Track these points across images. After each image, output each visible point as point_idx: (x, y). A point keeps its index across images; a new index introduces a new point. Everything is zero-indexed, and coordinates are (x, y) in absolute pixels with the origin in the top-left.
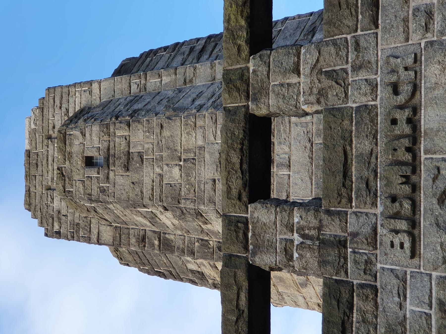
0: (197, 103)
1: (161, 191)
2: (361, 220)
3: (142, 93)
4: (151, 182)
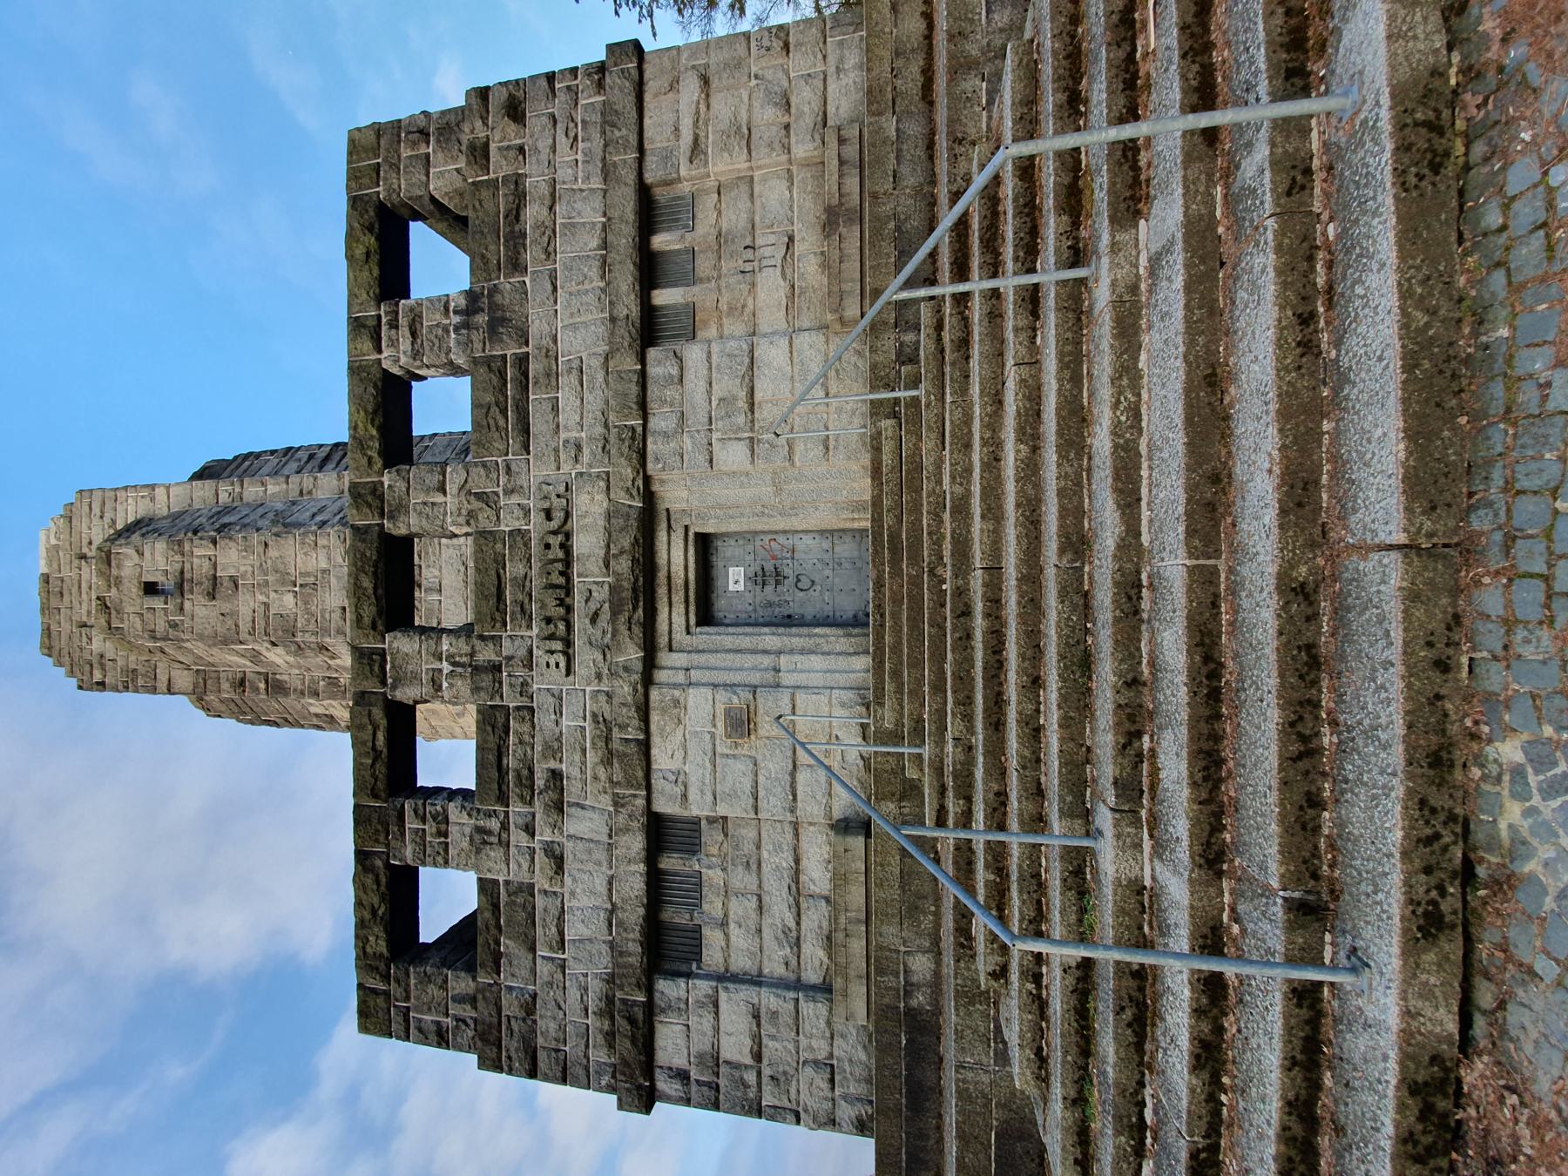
0: (319, 518)
1: (267, 623)
2: (516, 643)
3: (235, 504)
4: (251, 613)
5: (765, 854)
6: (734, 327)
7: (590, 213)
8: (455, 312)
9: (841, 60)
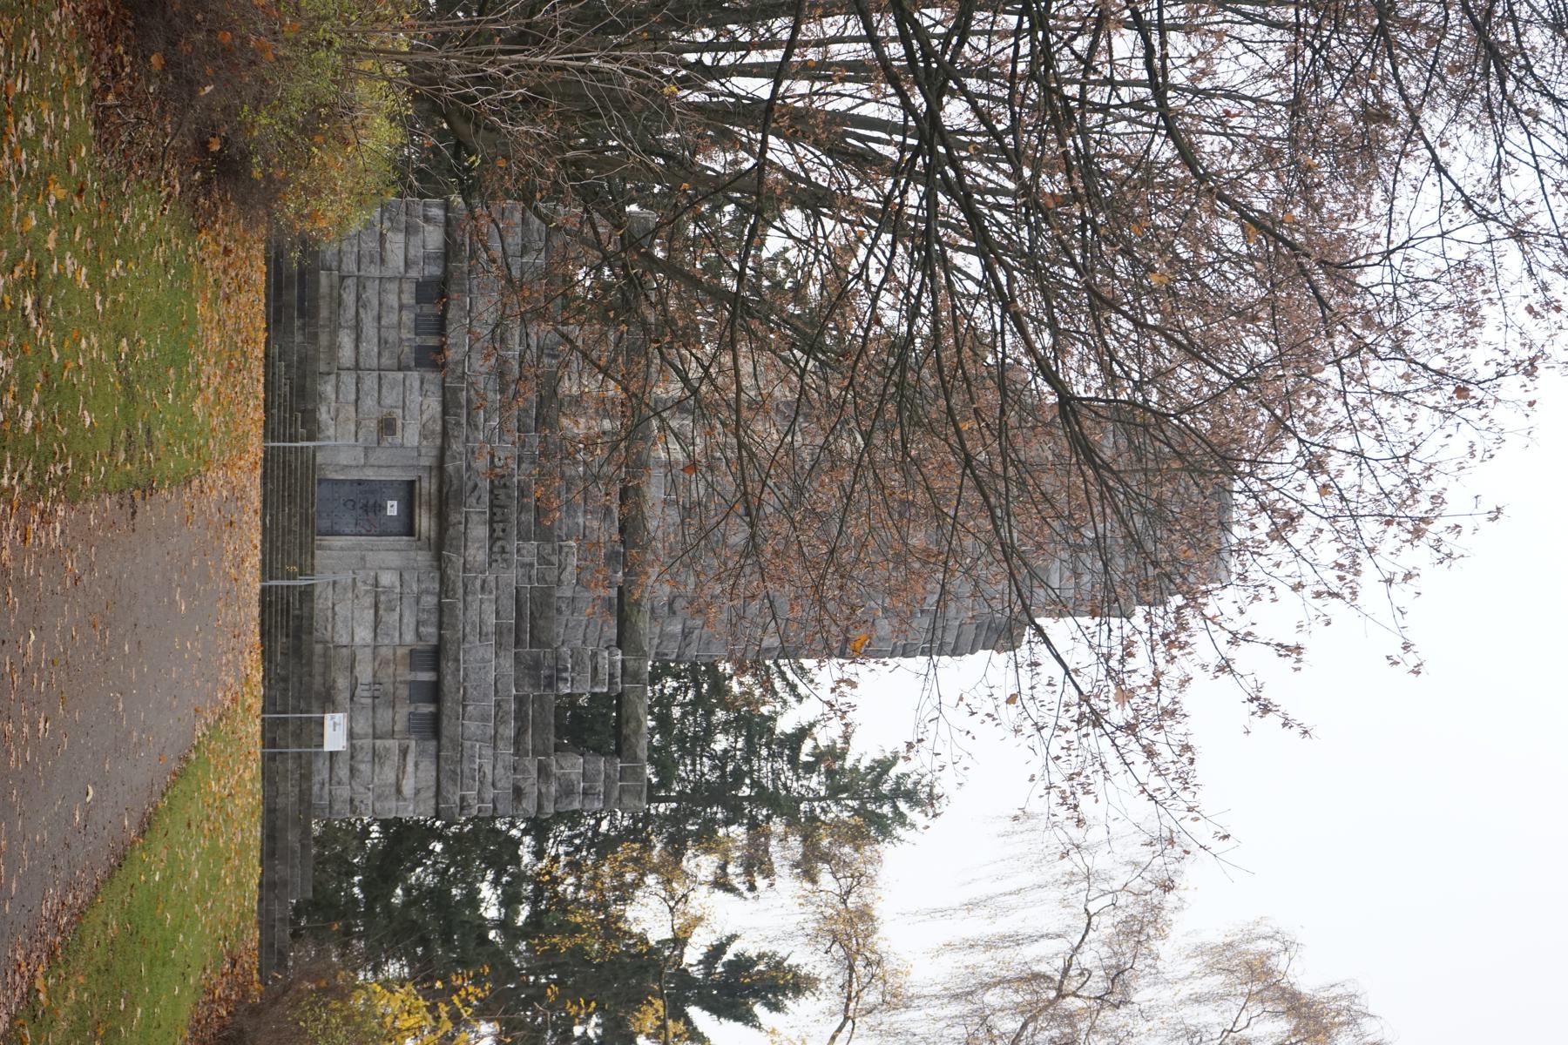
5: (376, 349)
6: (385, 652)
7: (472, 727)
8: (566, 679)
9: (322, 788)
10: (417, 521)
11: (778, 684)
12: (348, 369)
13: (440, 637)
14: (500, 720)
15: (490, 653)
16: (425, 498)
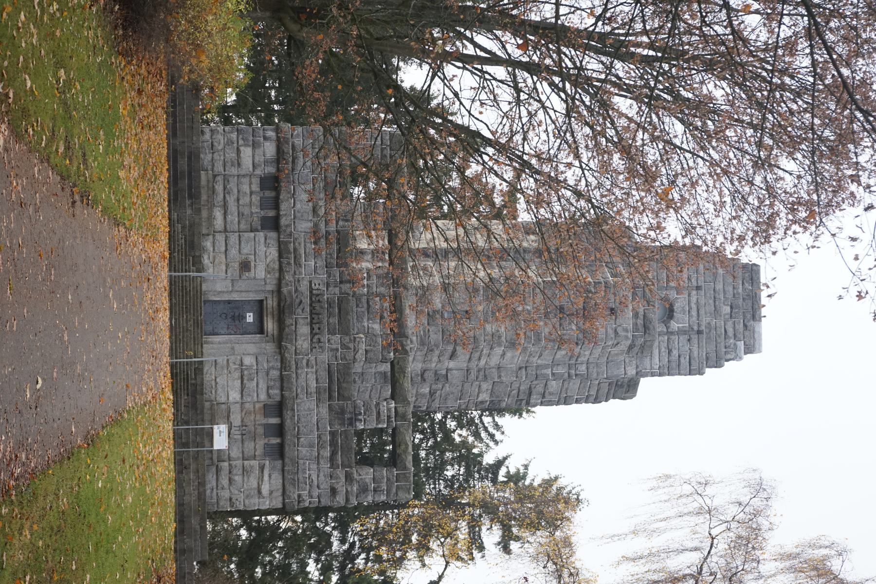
5: (237, 219)
7: (304, 451)
8: (361, 420)
9: (212, 492)
10: (265, 324)
11: (483, 434)
12: (220, 232)
13: (282, 396)
14: (320, 446)
15: (313, 405)
16: (270, 310)
